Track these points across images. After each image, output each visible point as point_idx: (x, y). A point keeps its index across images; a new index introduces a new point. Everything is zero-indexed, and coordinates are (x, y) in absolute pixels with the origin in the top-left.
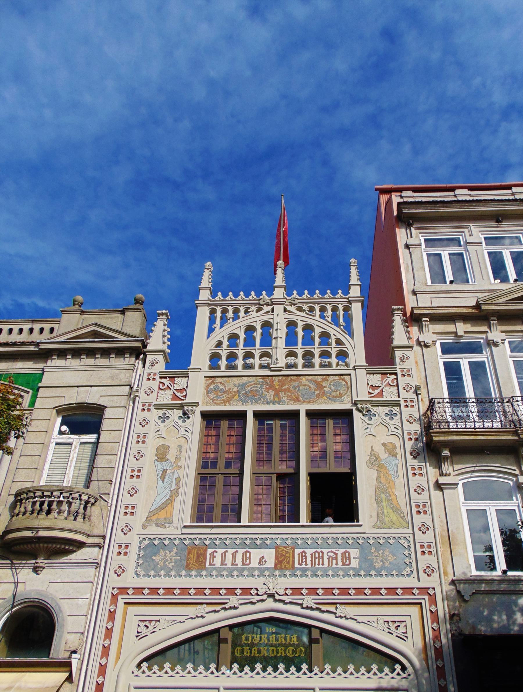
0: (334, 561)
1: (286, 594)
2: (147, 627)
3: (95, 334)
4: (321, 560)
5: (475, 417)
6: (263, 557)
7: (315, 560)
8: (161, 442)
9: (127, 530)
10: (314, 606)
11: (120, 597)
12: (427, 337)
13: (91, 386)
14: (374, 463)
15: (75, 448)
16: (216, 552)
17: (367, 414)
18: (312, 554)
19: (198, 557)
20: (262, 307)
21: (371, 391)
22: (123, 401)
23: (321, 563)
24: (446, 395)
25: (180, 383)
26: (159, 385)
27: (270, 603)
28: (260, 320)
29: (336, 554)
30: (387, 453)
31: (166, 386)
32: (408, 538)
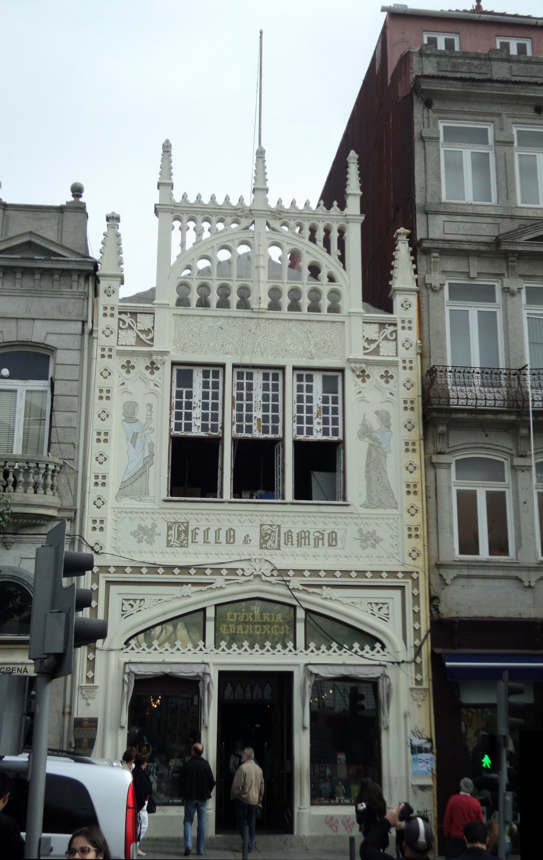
0: (320, 542)
1: (272, 575)
2: (132, 606)
3: (30, 245)
4: (307, 540)
5: (478, 392)
6: (248, 536)
7: (301, 540)
8: (128, 398)
9: (100, 503)
10: (301, 588)
11: (101, 575)
12: (435, 279)
13: (34, 319)
14: (366, 434)
15: (21, 396)
16: (198, 529)
17: (361, 374)
18: (298, 534)
19: (179, 533)
20: (240, 219)
21: (366, 346)
22: (76, 342)
23: (307, 543)
24: (449, 363)
25: (144, 322)
26: (119, 323)
27: (256, 585)
28: (237, 239)
29: (323, 534)
30: (380, 423)
31: (127, 325)
32: (396, 520)
